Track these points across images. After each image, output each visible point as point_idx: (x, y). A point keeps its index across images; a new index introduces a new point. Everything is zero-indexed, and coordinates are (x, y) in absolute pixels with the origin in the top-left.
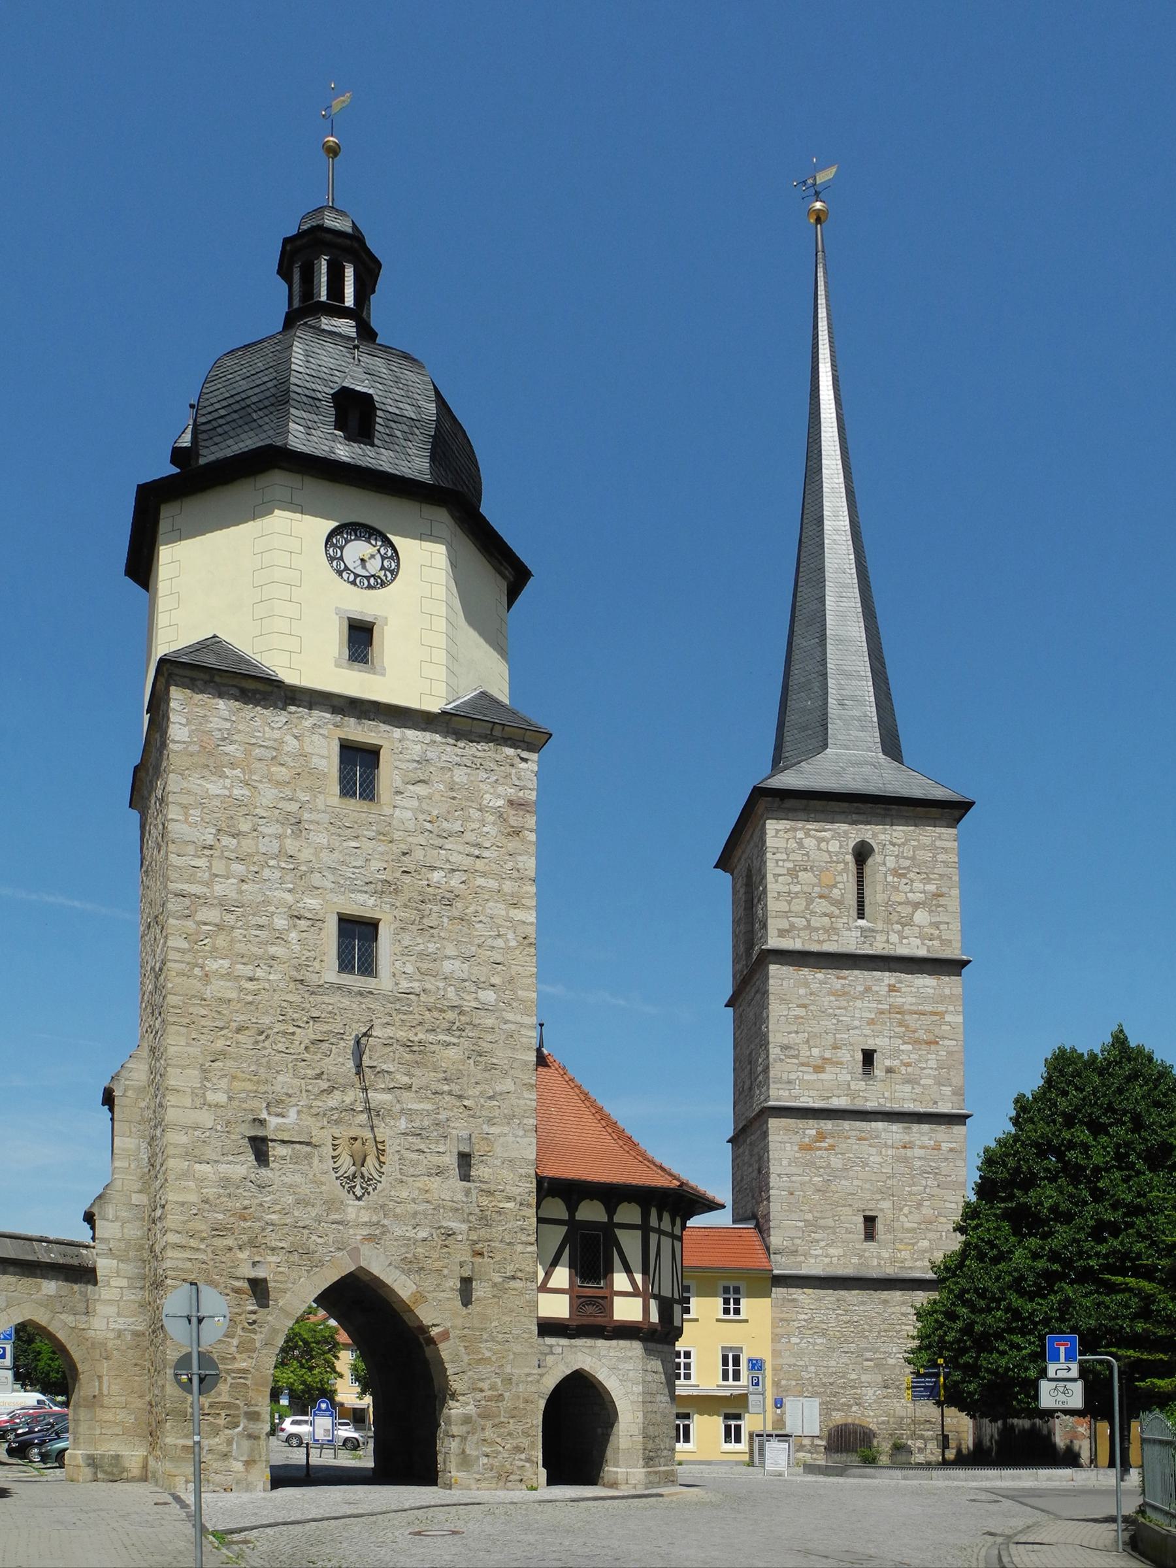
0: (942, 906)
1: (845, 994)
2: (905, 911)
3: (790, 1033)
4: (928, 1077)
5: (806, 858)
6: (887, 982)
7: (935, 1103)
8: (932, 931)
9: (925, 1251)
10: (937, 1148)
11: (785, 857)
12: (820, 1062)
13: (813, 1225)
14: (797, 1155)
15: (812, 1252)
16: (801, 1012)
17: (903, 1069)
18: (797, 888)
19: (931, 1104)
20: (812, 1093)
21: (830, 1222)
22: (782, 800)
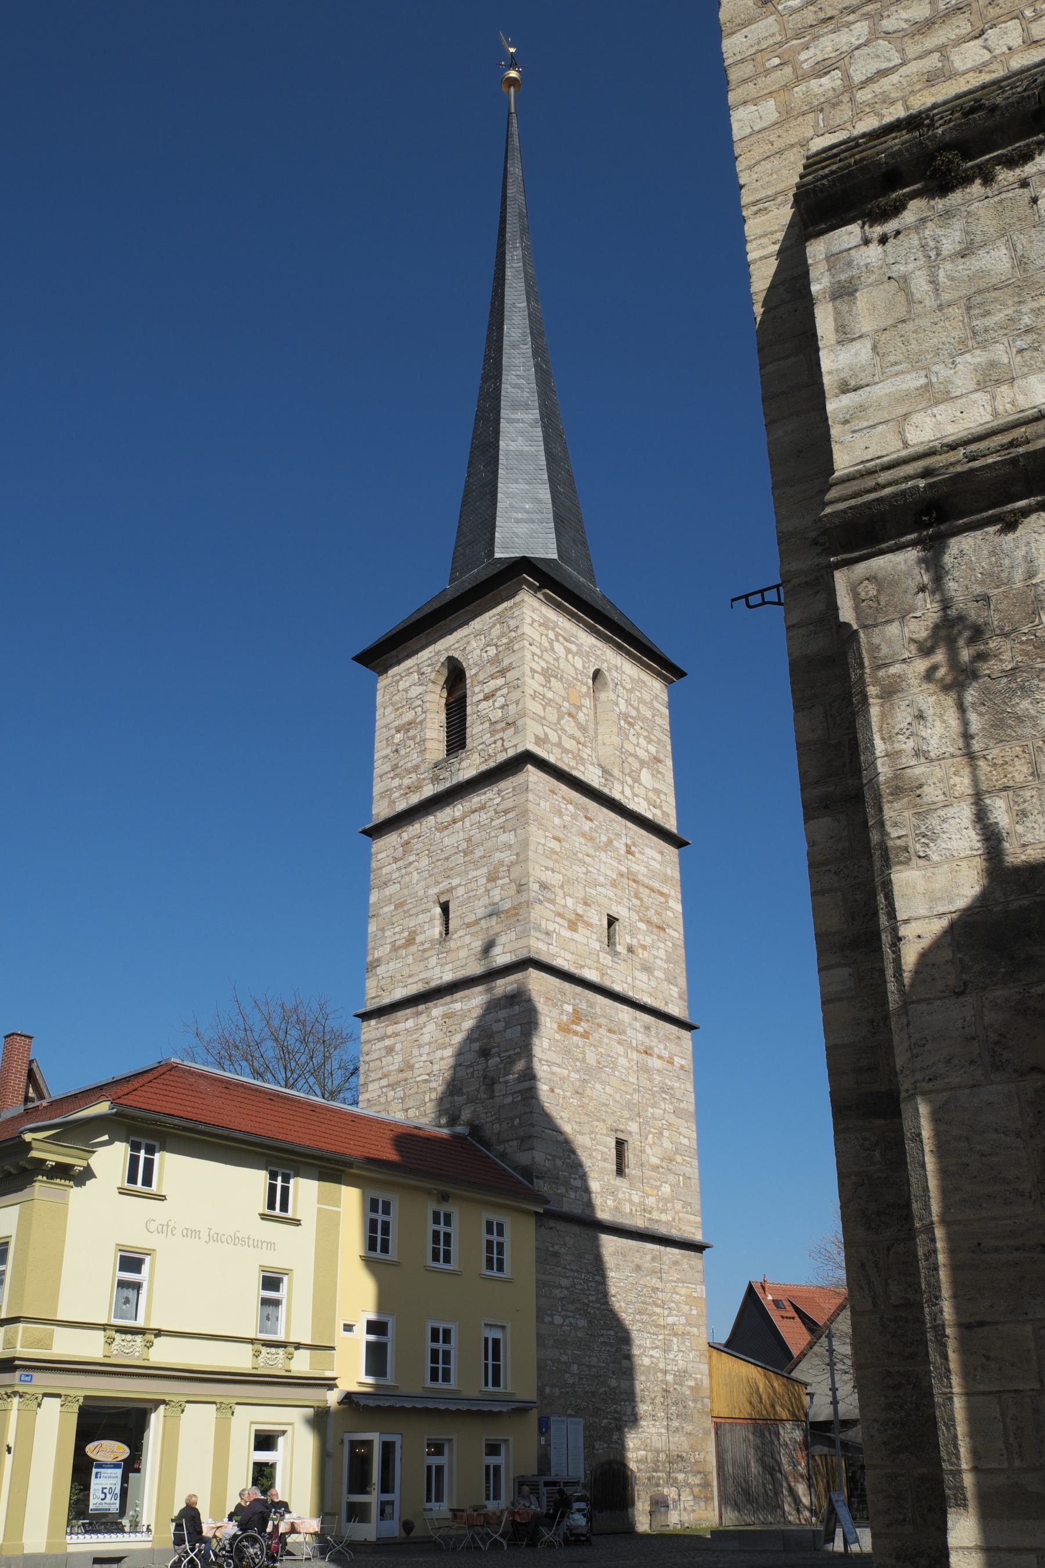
0: (660, 773)
1: (592, 839)
3: (547, 868)
12: (573, 917)
14: (558, 1037)
19: (663, 1003)
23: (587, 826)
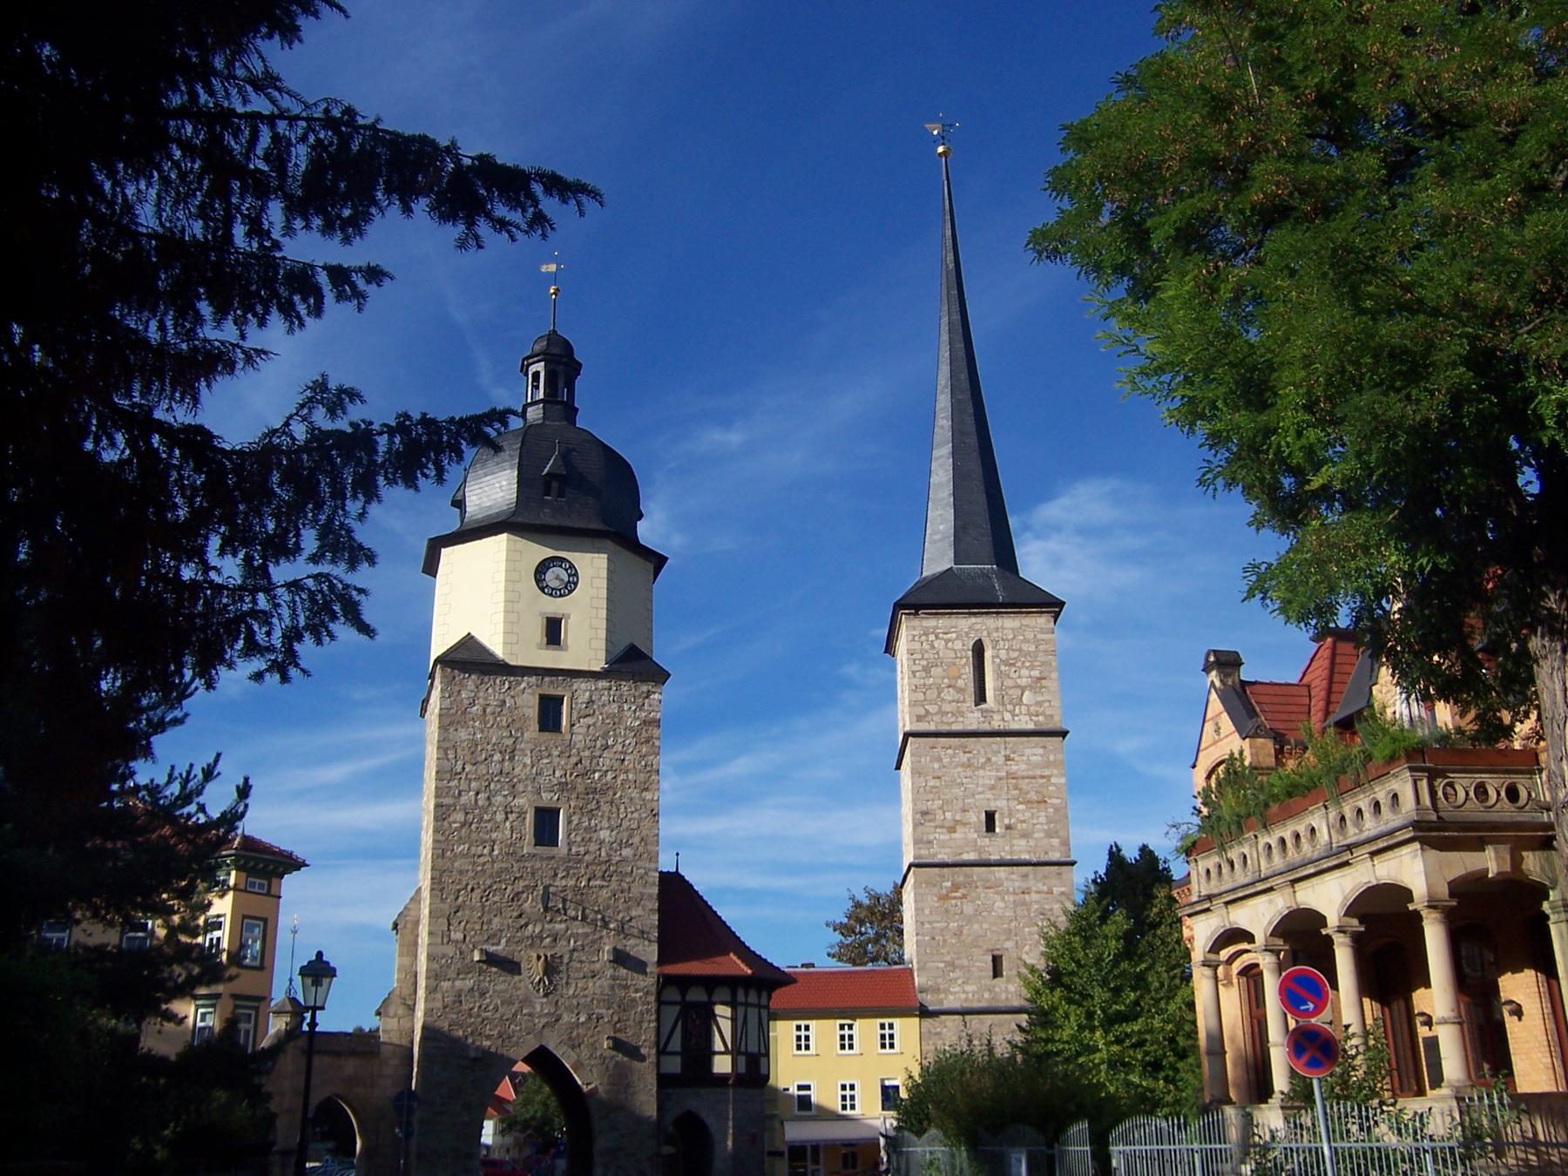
2: (1015, 693)
10: (1050, 892)
13: (952, 965)
23: (964, 758)
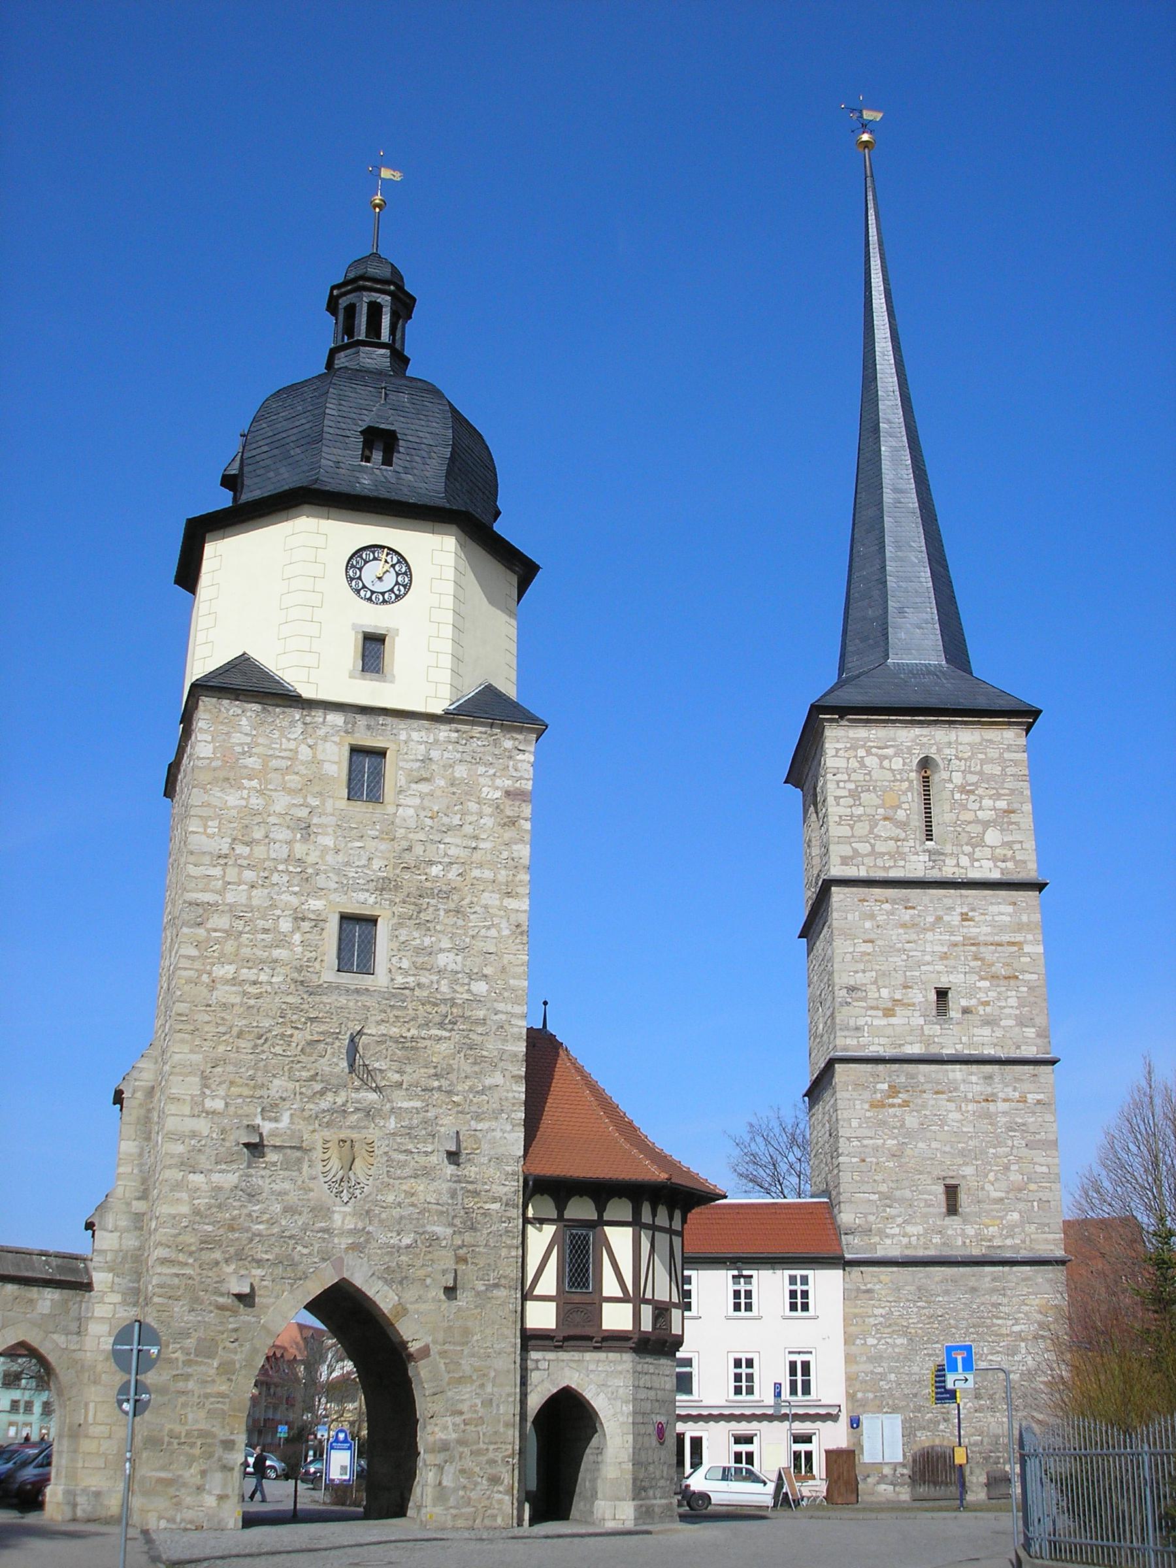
2: (975, 829)
3: (857, 972)
4: (1009, 1016)
5: (867, 778)
6: (959, 910)
7: (1018, 1047)
8: (1005, 852)
9: (1015, 1226)
11: (846, 777)
12: (890, 1005)
14: (868, 1114)
15: (888, 1231)
16: (868, 948)
17: (981, 1008)
18: (860, 811)
19: (1014, 1047)
20: (883, 1041)
21: (907, 1194)
22: (841, 717)
23: (907, 916)
